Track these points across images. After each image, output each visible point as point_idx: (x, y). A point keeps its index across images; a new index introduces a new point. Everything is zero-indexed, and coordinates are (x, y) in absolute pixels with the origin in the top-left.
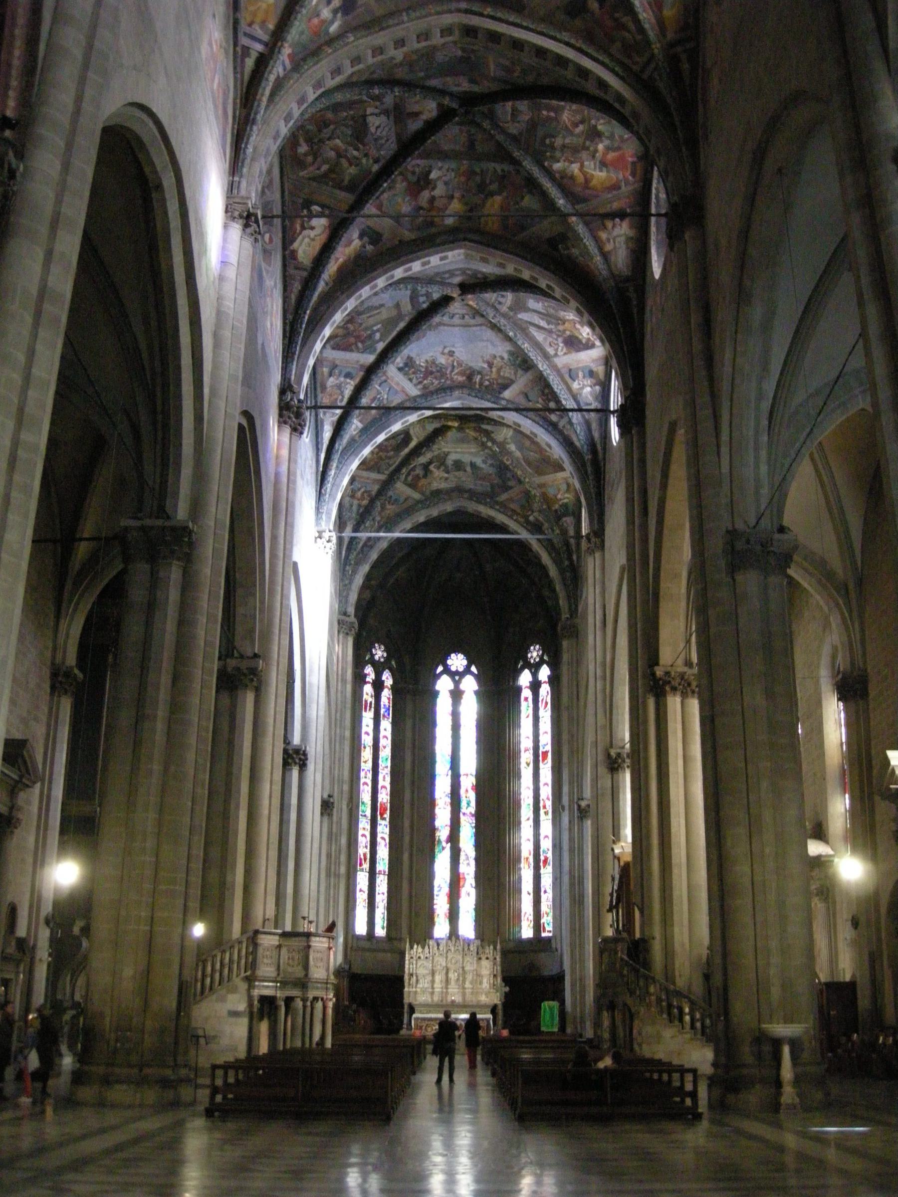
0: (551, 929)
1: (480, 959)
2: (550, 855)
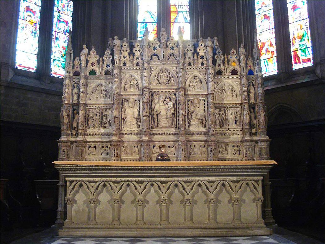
0: (310, 56)
1: (220, 73)
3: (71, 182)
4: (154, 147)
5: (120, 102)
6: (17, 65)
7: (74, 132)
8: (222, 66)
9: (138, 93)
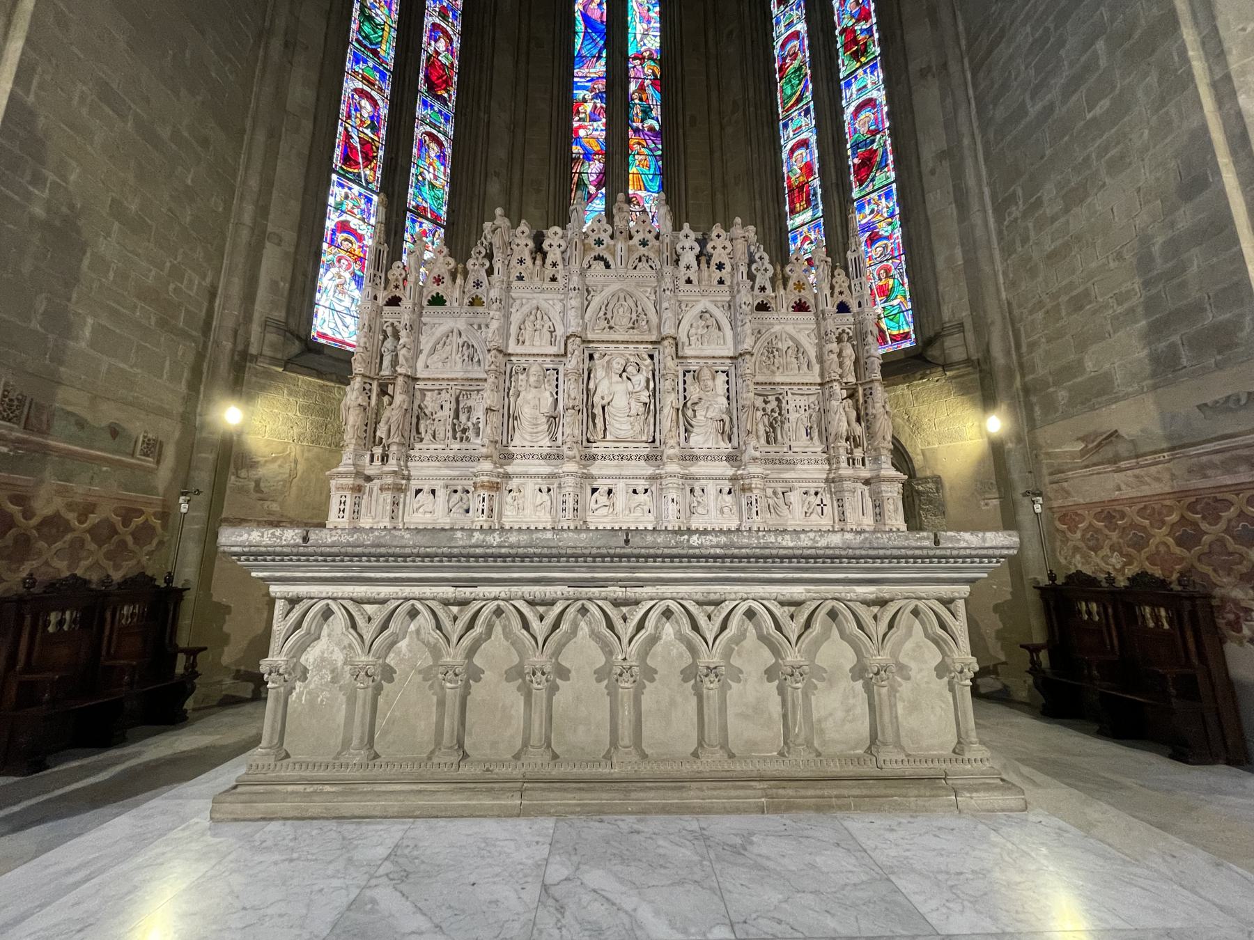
1: (762, 307)
2: (883, 142)
3: (293, 601)
4: (594, 490)
5: (507, 371)
6: (313, 333)
7: (378, 451)
8: (769, 291)
9: (553, 350)
